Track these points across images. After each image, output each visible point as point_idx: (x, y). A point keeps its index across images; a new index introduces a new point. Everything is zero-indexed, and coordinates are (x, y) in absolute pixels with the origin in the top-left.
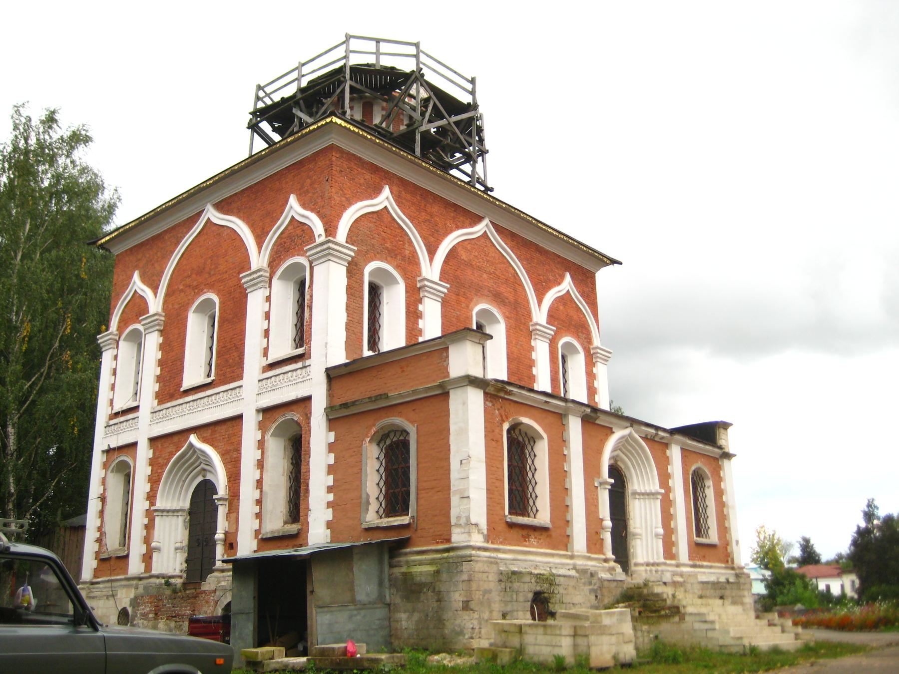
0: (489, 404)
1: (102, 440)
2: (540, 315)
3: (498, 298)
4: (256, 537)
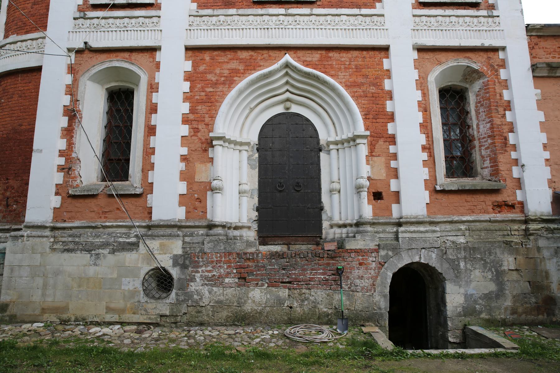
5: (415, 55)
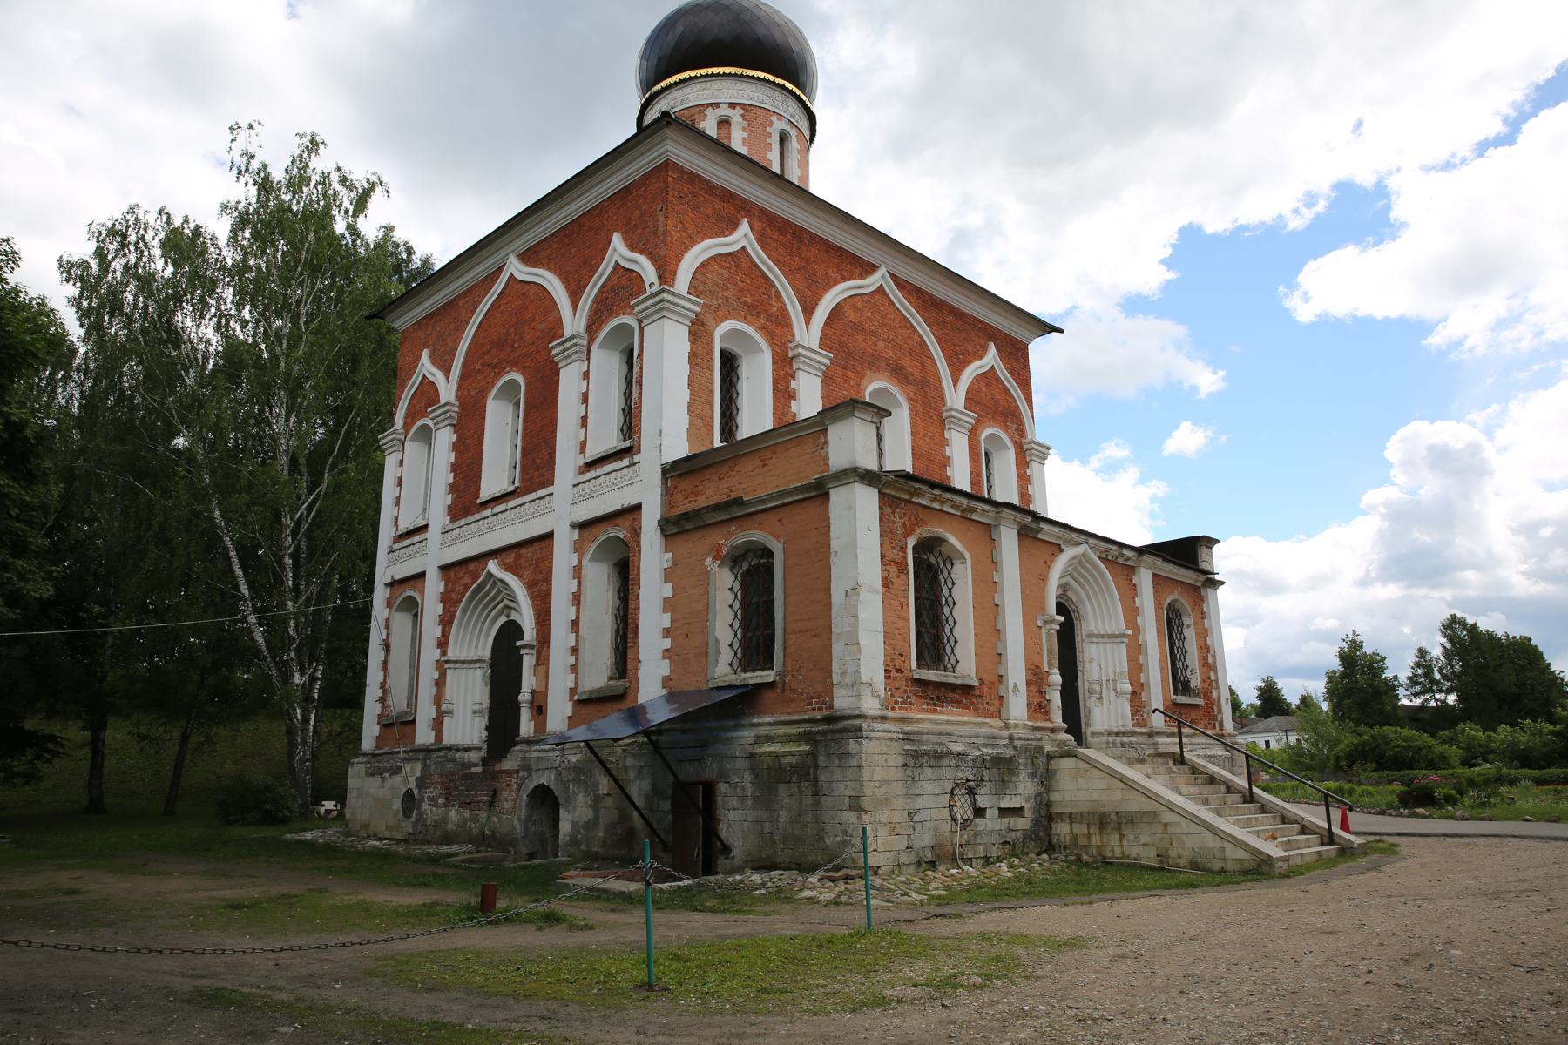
0: (888, 510)
1: (385, 570)
2: (956, 398)
3: (898, 373)
4: (571, 698)
5: (576, 534)
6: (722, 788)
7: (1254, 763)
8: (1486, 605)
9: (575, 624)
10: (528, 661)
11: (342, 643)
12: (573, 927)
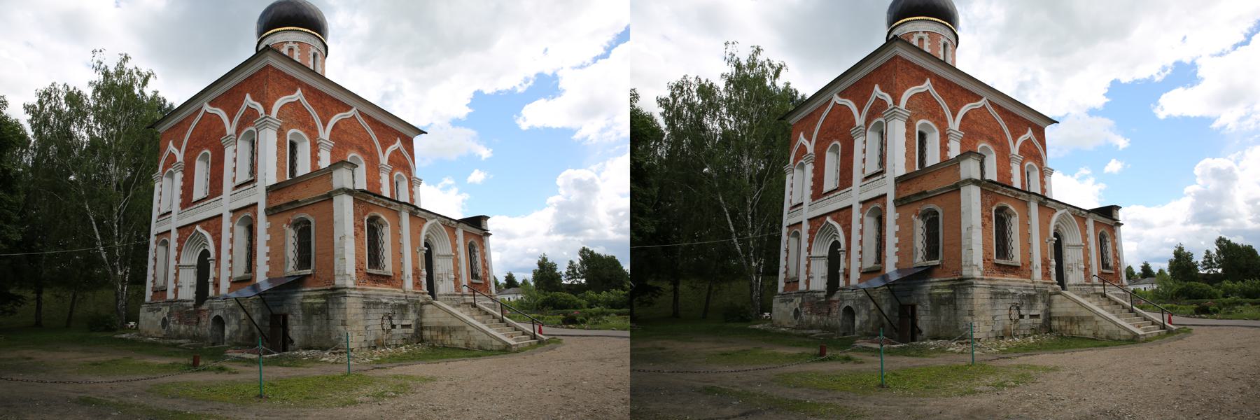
3: (361, 150)
6: (290, 317)
7: (504, 307)
8: (597, 243)
9: (231, 251)
10: (212, 266)
11: (138, 258)
12: (230, 373)
